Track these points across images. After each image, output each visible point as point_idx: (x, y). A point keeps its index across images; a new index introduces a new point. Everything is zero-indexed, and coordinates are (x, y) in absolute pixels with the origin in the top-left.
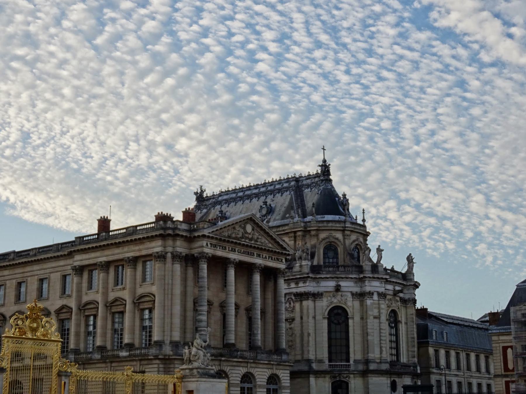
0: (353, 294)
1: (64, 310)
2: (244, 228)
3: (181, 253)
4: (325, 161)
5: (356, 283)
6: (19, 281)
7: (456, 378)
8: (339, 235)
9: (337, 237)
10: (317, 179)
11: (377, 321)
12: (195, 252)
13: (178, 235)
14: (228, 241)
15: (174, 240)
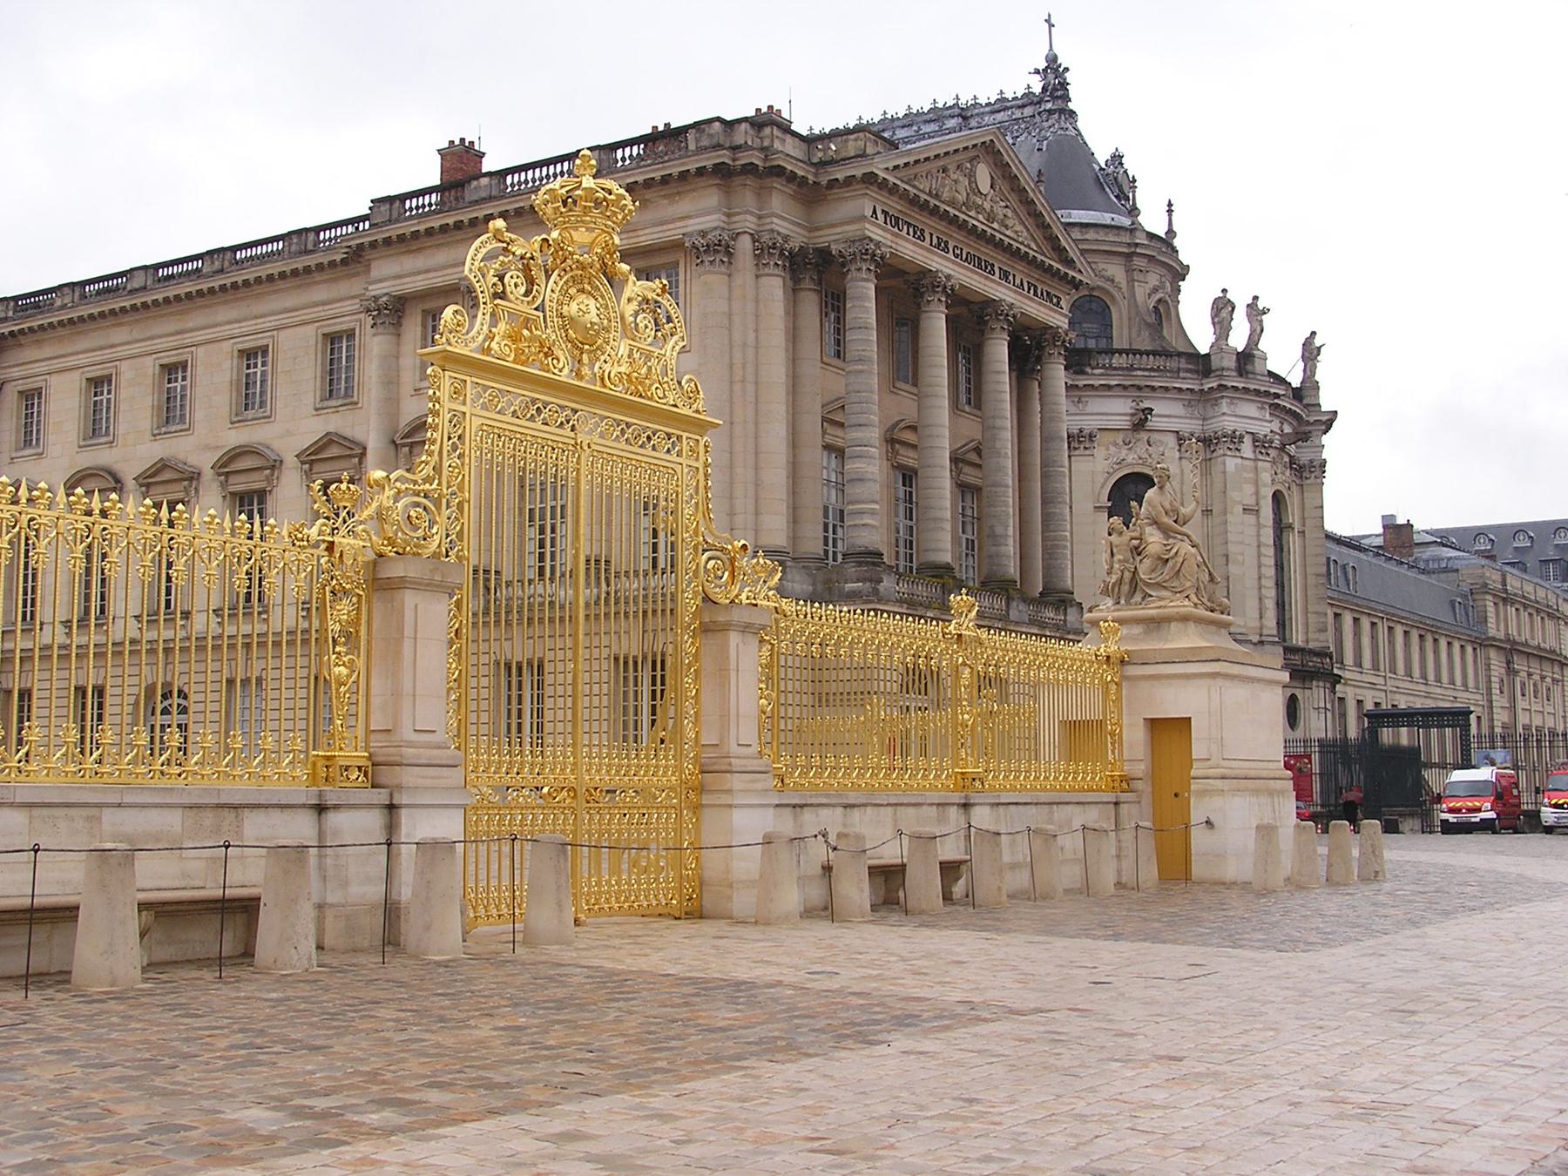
0: (1180, 439)
1: (334, 451)
2: (971, 176)
3: (786, 238)
4: (1052, 59)
5: (1189, 404)
6: (165, 361)
7: (1373, 693)
8: (1116, 270)
9: (1109, 273)
10: (1028, 111)
11: (1251, 519)
12: (833, 238)
13: (778, 171)
14: (934, 212)
15: (762, 194)
